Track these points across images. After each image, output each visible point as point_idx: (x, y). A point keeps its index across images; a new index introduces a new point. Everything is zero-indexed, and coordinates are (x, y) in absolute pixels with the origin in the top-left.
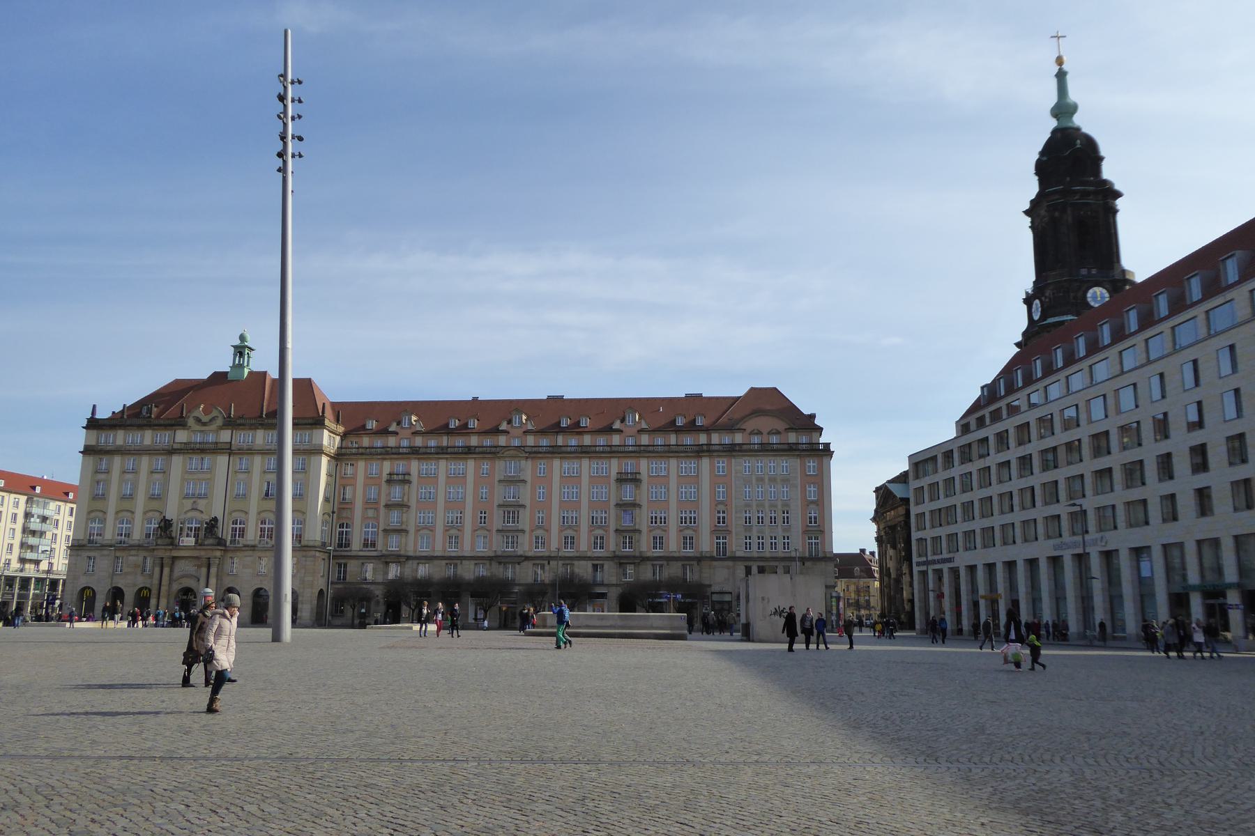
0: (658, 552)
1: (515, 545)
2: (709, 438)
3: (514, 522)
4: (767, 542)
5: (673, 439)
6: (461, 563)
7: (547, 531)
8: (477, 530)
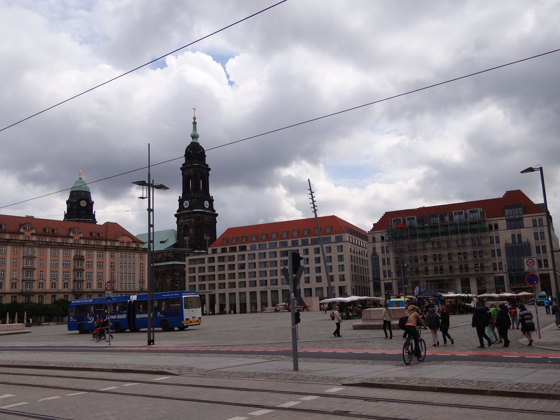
0: (89, 290)
1: (31, 287)
2: (106, 243)
3: (30, 276)
4: (128, 285)
5: (92, 243)
6: (5, 296)
7: (44, 280)
8: (12, 280)
